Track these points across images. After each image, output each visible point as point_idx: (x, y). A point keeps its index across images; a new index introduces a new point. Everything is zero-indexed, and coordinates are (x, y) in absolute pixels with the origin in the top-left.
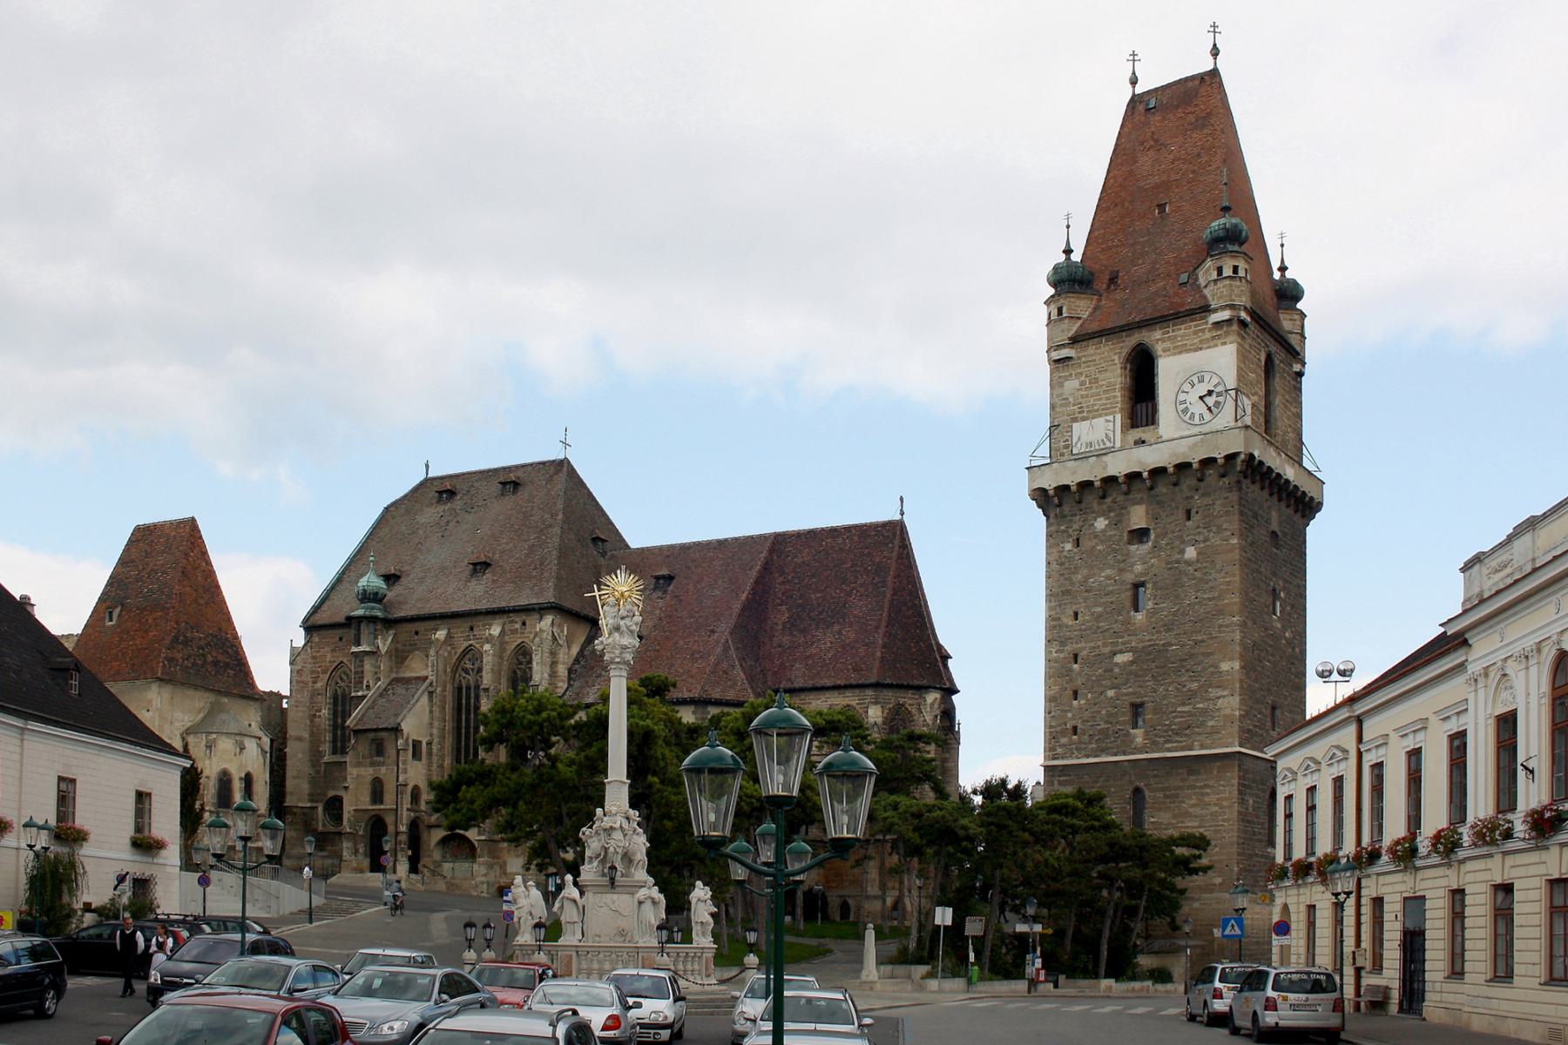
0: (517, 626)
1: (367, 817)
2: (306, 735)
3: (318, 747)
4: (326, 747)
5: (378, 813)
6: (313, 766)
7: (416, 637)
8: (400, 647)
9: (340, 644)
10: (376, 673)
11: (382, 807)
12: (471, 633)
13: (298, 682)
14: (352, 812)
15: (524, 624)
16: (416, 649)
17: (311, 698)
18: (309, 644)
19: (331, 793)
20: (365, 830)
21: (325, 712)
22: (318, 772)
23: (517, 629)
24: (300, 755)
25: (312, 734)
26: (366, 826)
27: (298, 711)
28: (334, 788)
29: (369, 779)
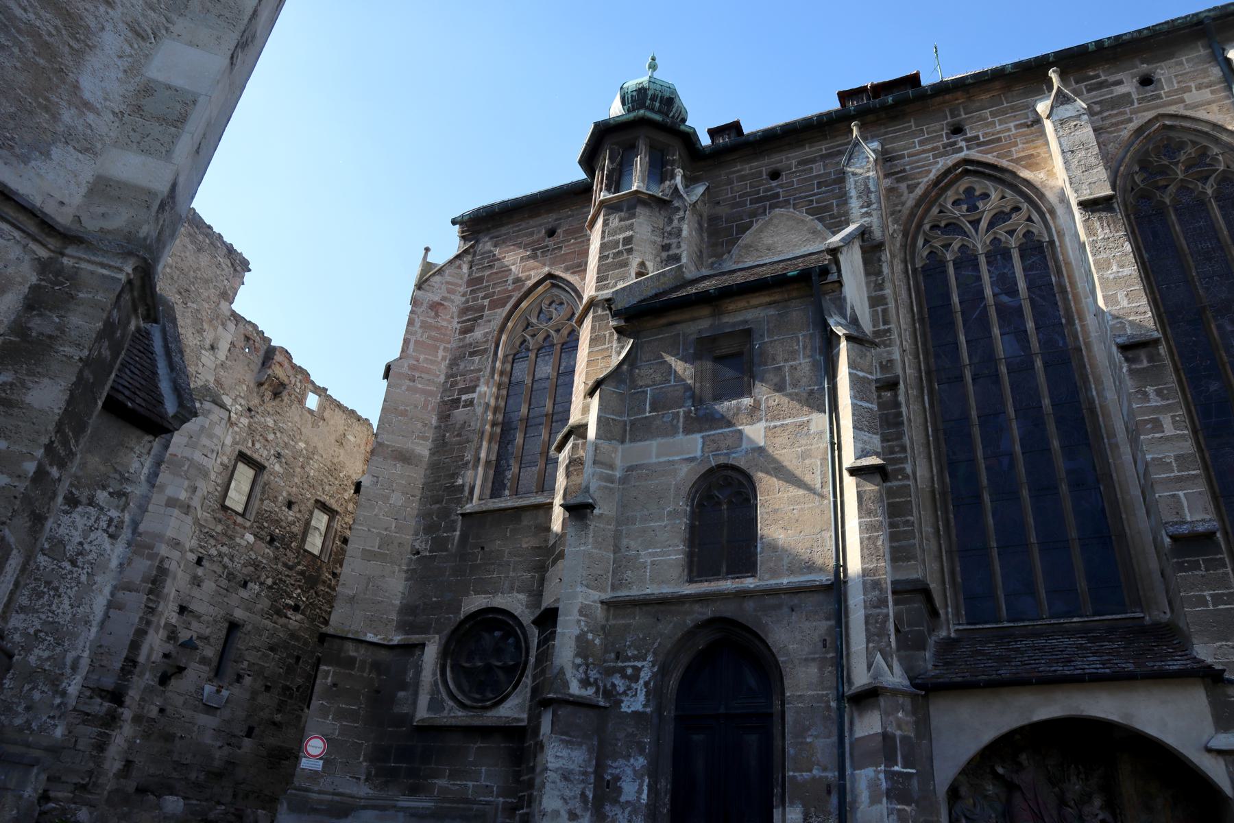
0: (1128, 86)
1: (670, 628)
2: (423, 450)
3: (454, 476)
4: (476, 478)
5: (728, 610)
6: (430, 529)
7: (774, 184)
8: (723, 210)
9: (550, 242)
10: (666, 248)
11: (750, 583)
12: (959, 138)
13: (425, 326)
14: (599, 612)
15: (1146, 81)
16: (772, 207)
17: (454, 363)
18: (469, 258)
19: (475, 603)
20: (655, 693)
21: (486, 391)
22: (439, 544)
23: (1129, 94)
24: (397, 499)
25: (440, 446)
26: (663, 671)
27: (409, 389)
28: (483, 587)
29: (685, 475)
